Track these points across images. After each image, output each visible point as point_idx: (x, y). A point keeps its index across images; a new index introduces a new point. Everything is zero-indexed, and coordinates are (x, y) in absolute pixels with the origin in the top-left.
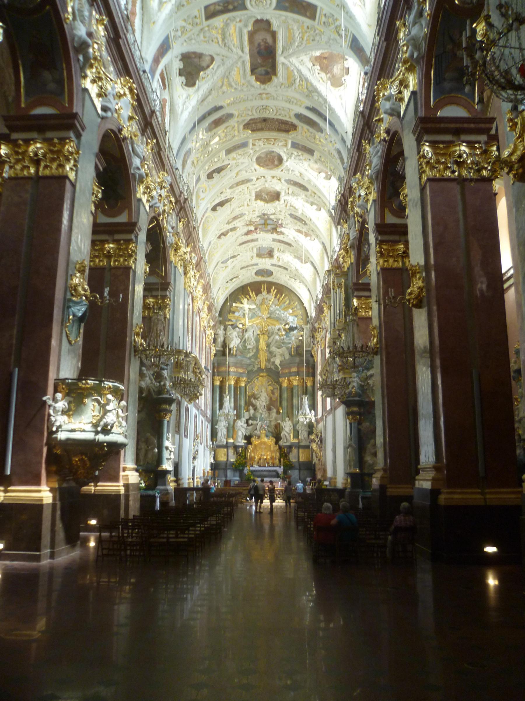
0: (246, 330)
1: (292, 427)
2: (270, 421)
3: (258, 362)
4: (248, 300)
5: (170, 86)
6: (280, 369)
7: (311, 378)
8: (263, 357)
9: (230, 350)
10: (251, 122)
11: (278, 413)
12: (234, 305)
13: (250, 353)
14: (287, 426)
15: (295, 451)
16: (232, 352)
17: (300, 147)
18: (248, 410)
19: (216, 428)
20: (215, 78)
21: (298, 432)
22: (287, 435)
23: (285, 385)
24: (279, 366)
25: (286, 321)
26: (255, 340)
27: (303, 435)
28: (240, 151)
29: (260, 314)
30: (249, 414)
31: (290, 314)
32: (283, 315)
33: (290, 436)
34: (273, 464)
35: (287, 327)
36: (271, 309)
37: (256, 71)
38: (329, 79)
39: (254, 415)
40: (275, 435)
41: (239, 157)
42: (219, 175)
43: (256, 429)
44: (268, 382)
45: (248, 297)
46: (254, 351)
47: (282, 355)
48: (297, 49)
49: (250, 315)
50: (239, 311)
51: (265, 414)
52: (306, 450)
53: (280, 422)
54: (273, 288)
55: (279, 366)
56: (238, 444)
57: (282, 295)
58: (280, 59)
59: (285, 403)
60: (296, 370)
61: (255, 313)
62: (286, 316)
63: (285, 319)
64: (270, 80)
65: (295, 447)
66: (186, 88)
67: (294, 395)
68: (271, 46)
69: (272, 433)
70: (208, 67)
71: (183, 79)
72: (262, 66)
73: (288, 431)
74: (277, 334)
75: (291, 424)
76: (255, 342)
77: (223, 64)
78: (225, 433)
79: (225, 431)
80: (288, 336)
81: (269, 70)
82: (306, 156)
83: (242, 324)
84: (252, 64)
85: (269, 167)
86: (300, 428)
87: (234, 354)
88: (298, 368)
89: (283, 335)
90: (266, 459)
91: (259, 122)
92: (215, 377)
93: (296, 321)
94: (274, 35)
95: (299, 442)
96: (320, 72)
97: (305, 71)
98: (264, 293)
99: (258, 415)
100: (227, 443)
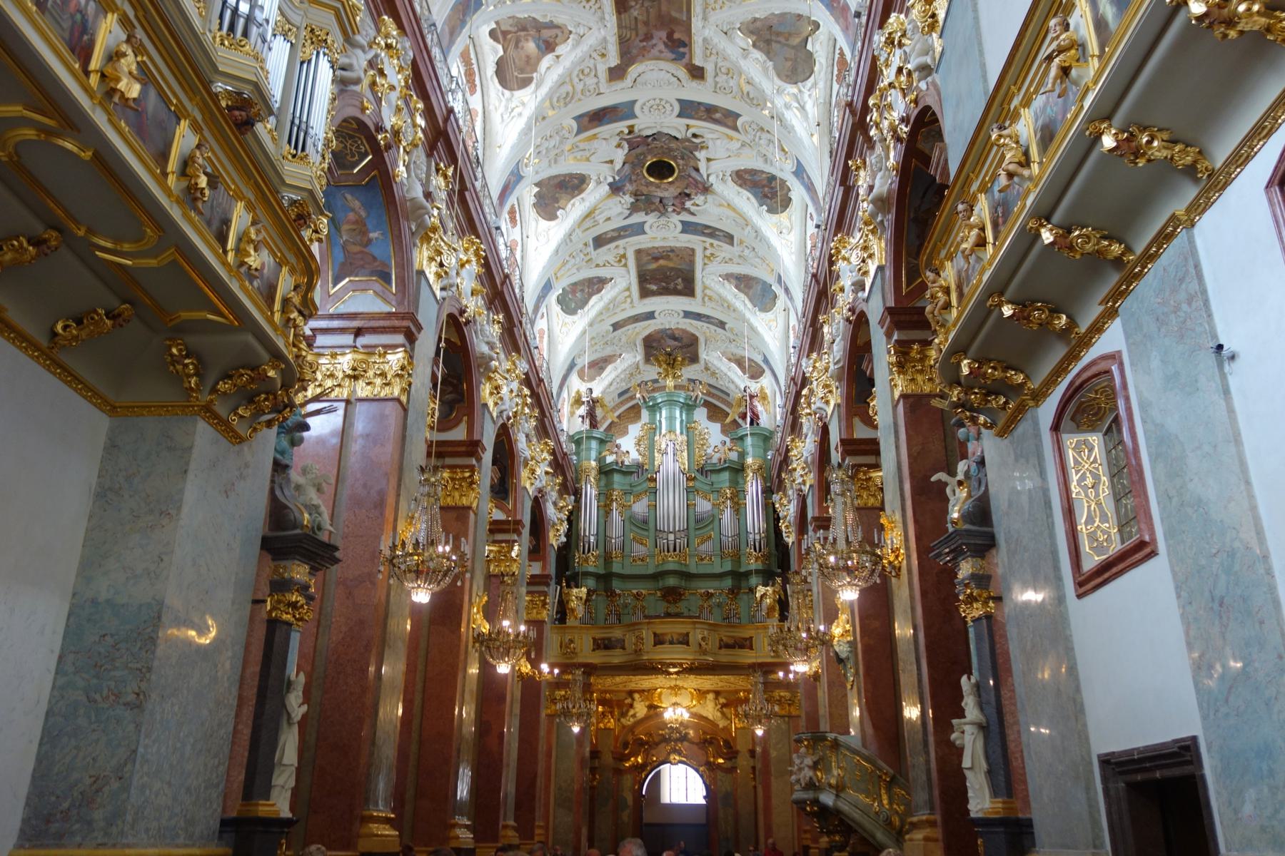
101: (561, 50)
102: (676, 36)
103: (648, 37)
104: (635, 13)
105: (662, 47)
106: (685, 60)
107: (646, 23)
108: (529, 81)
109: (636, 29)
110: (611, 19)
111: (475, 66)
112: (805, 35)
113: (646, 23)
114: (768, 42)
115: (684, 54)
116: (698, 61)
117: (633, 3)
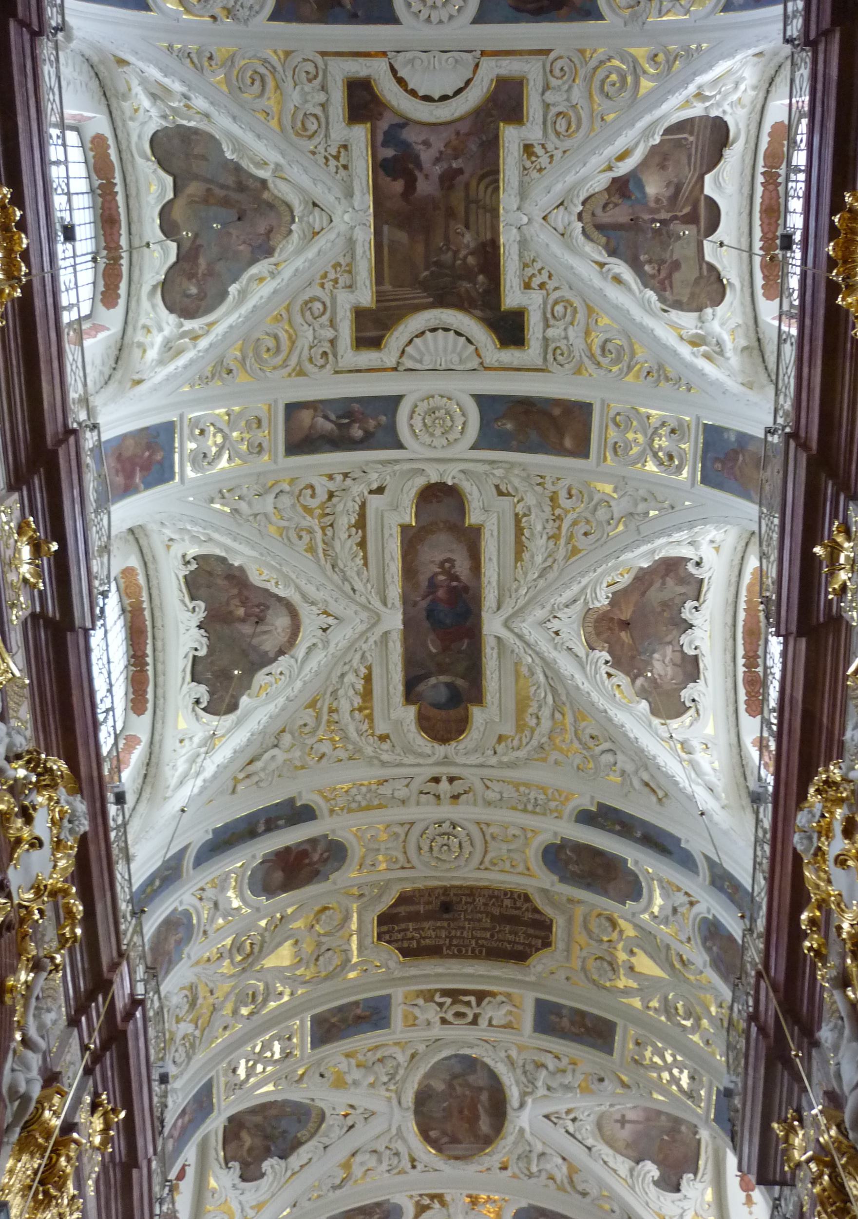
5: (159, 713)
10: (402, 910)
17: (565, 1022)
20: (299, 684)
28: (362, 1042)
37: (421, 687)
38: (643, 694)
41: (357, 1074)
42: (282, 1163)
48: (541, 583)
58: (492, 625)
64: (461, 726)
66: (206, 717)
68: (466, 589)
70: (281, 652)
71: (202, 691)
72: (442, 669)
77: (326, 644)
81: (460, 682)
82: (587, 1057)
84: (409, 661)
85: (459, 1149)
91: (429, 916)
94: (471, 540)
96: (612, 671)
97: (566, 666)
101: (601, 182)
102: (398, 186)
103: (449, 179)
104: (468, 238)
105: (426, 156)
106: (384, 125)
107: (450, 213)
108: (668, 131)
109: (468, 201)
110: (508, 238)
111: (760, 169)
112: (181, 202)
113: (450, 213)
114: (241, 187)
115: (385, 144)
116: (360, 134)
117: (471, 260)
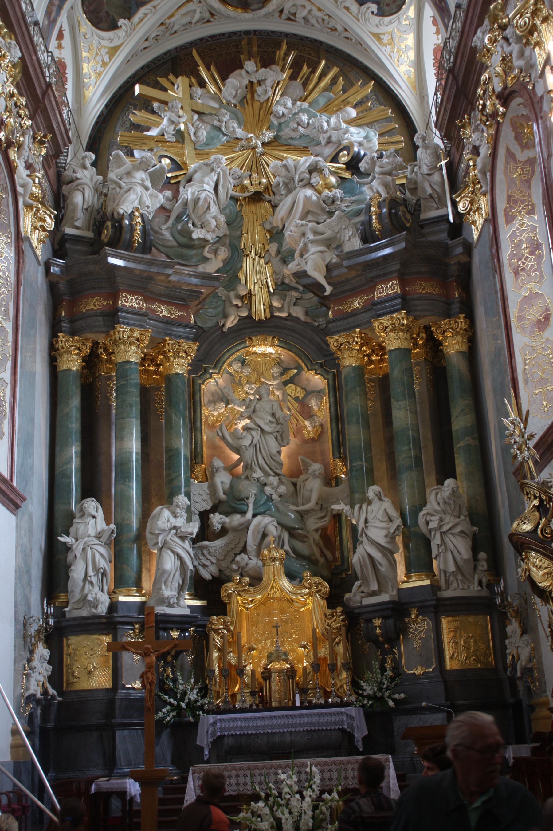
0: (190, 180)
1: (399, 521)
2: (302, 515)
3: (242, 298)
4: (190, 86)
6: (329, 290)
7: (461, 322)
8: (257, 276)
9: (118, 221)
11: (331, 480)
12: (137, 89)
13: (206, 260)
14: (376, 520)
15: (419, 626)
16: (126, 236)
18: (208, 477)
19: (67, 548)
21: (427, 543)
22: (377, 555)
23: (350, 360)
24: (324, 282)
25: (339, 142)
26: (221, 211)
27: (452, 550)
29: (240, 132)
30: (213, 490)
31: (351, 122)
32: (325, 125)
33: (393, 564)
34: (327, 695)
35: (344, 157)
36: (281, 110)
39: (231, 491)
40: (326, 573)
43: (244, 550)
44: (285, 370)
45: (193, 80)
46: (224, 253)
47: (332, 243)
49: (203, 134)
50: (157, 125)
51: (275, 488)
52: (471, 619)
53: (340, 507)
54: (284, 47)
55: (324, 282)
56: (160, 610)
57: (314, 68)
59: (355, 433)
60: (398, 289)
61: (219, 129)
62: (337, 128)
63: (334, 139)
65: (422, 611)
67: (396, 388)
69: (311, 561)
73: (382, 541)
74: (309, 185)
75: (394, 513)
76: (222, 219)
78: (109, 569)
79: (102, 556)
80: (350, 192)
83: (171, 159)
86: (433, 525)
87: (138, 237)
88: (403, 283)
89: (329, 187)
90: (292, 672)
92: (63, 340)
93: (375, 140)
95: (435, 588)
98: (250, 65)
99: (251, 490)
100: (113, 607)
